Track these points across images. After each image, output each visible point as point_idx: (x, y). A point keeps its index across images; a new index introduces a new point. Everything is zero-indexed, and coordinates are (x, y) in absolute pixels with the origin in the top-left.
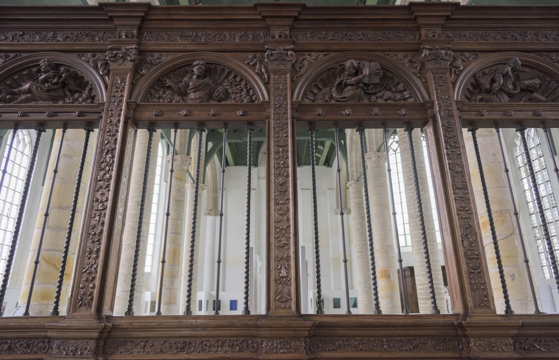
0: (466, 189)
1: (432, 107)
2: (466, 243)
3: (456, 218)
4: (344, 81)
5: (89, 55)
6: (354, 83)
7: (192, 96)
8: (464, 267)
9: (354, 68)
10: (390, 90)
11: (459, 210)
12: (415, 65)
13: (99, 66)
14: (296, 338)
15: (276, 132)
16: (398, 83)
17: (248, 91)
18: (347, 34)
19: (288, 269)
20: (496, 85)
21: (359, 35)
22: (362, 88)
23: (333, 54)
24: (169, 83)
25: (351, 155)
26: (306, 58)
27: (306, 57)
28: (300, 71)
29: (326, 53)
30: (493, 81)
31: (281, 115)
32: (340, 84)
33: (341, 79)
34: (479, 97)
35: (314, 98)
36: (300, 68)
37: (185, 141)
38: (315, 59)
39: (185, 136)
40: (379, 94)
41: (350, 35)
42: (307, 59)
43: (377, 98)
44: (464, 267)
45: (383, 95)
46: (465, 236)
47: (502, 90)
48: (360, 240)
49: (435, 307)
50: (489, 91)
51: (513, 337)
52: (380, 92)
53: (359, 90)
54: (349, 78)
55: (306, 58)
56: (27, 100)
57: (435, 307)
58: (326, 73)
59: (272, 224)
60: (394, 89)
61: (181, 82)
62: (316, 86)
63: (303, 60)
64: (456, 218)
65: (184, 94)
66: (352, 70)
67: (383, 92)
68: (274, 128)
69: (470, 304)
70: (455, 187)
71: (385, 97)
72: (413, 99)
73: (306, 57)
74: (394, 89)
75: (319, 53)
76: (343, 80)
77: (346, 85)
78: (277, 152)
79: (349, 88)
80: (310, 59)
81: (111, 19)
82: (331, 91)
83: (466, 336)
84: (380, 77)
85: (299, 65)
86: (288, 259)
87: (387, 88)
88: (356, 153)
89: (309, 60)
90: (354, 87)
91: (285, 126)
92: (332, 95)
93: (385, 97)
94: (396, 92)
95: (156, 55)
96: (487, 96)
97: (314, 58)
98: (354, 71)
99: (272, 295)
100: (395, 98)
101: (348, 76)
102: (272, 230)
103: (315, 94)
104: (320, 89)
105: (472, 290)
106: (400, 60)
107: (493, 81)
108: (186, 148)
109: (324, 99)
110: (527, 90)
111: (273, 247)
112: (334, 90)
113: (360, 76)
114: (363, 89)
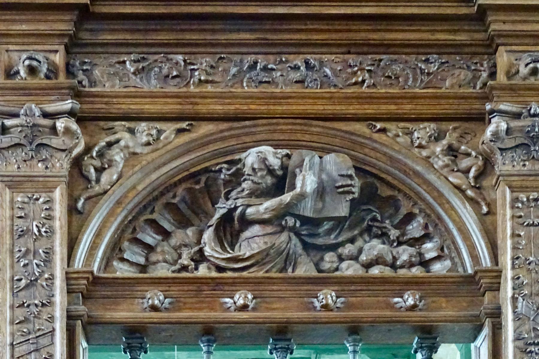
1: (496, 287)
4: (239, 210)
6: (266, 216)
9: (271, 171)
10: (383, 236)
12: (464, 163)
15: (17, 355)
16: (410, 217)
18: (256, 63)
21: (296, 68)
22: (292, 229)
23: (206, 128)
26: (118, 141)
27: (117, 136)
28: (98, 181)
29: (184, 125)
31: (33, 309)
32: (227, 218)
33: (230, 204)
35: (147, 259)
36: (100, 171)
38: (148, 144)
40: (348, 249)
41: (265, 69)
42: (122, 143)
43: (341, 259)
45: (360, 251)
52: (352, 241)
53: (284, 237)
54: (253, 200)
55: (118, 141)
58: (184, 186)
60: (394, 233)
62: (154, 224)
63: (110, 145)
66: (262, 177)
67: (359, 243)
68: (12, 345)
71: (363, 258)
72: (448, 263)
73: (117, 136)
74: (394, 233)
75: (159, 125)
76: (236, 208)
79: (256, 229)
80: (131, 144)
82: (199, 242)
84: (350, 197)
85: (97, 163)
87: (375, 229)
89: (127, 147)
90: (269, 229)
91: (44, 341)
92: (201, 251)
93: (363, 258)
94: (400, 244)
97: (145, 139)
98: (269, 180)
100: (395, 259)
101: (250, 195)
103: (150, 248)
104: (166, 235)
106: (420, 146)
109: (175, 262)
112: (208, 235)
113: (287, 197)
114: (298, 235)
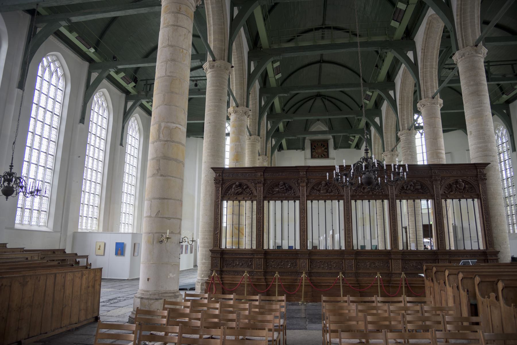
0: (395, 219)
2: (394, 233)
3: (392, 227)
5: (293, 180)
7: (322, 192)
8: (392, 239)
11: (393, 225)
13: (296, 183)
14: (352, 254)
17: (337, 190)
19: (350, 239)
20: (408, 188)
24: (315, 188)
25: (374, 147)
30: (407, 187)
34: (403, 191)
37: (264, 145)
39: (264, 142)
40: (375, 191)
44: (392, 239)
46: (394, 232)
47: (409, 189)
48: (380, 208)
49: (385, 248)
50: (406, 190)
51: (401, 254)
56: (277, 193)
57: (385, 248)
59: (346, 228)
61: (318, 187)
64: (392, 227)
65: (319, 191)
69: (393, 247)
70: (392, 219)
77: (365, 188)
78: (347, 210)
81: (298, 169)
83: (391, 254)
86: (350, 237)
88: (378, 146)
95: (312, 180)
96: (406, 191)
99: (347, 245)
102: (346, 230)
105: (394, 244)
107: (407, 187)
108: (265, 151)
110: (417, 189)
111: (346, 234)
112: (362, 189)
